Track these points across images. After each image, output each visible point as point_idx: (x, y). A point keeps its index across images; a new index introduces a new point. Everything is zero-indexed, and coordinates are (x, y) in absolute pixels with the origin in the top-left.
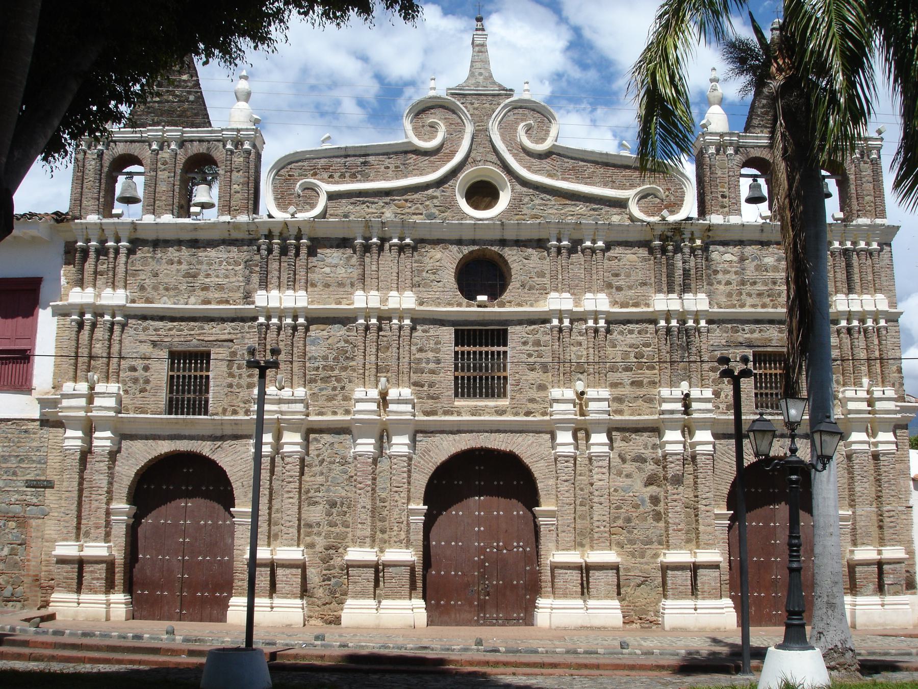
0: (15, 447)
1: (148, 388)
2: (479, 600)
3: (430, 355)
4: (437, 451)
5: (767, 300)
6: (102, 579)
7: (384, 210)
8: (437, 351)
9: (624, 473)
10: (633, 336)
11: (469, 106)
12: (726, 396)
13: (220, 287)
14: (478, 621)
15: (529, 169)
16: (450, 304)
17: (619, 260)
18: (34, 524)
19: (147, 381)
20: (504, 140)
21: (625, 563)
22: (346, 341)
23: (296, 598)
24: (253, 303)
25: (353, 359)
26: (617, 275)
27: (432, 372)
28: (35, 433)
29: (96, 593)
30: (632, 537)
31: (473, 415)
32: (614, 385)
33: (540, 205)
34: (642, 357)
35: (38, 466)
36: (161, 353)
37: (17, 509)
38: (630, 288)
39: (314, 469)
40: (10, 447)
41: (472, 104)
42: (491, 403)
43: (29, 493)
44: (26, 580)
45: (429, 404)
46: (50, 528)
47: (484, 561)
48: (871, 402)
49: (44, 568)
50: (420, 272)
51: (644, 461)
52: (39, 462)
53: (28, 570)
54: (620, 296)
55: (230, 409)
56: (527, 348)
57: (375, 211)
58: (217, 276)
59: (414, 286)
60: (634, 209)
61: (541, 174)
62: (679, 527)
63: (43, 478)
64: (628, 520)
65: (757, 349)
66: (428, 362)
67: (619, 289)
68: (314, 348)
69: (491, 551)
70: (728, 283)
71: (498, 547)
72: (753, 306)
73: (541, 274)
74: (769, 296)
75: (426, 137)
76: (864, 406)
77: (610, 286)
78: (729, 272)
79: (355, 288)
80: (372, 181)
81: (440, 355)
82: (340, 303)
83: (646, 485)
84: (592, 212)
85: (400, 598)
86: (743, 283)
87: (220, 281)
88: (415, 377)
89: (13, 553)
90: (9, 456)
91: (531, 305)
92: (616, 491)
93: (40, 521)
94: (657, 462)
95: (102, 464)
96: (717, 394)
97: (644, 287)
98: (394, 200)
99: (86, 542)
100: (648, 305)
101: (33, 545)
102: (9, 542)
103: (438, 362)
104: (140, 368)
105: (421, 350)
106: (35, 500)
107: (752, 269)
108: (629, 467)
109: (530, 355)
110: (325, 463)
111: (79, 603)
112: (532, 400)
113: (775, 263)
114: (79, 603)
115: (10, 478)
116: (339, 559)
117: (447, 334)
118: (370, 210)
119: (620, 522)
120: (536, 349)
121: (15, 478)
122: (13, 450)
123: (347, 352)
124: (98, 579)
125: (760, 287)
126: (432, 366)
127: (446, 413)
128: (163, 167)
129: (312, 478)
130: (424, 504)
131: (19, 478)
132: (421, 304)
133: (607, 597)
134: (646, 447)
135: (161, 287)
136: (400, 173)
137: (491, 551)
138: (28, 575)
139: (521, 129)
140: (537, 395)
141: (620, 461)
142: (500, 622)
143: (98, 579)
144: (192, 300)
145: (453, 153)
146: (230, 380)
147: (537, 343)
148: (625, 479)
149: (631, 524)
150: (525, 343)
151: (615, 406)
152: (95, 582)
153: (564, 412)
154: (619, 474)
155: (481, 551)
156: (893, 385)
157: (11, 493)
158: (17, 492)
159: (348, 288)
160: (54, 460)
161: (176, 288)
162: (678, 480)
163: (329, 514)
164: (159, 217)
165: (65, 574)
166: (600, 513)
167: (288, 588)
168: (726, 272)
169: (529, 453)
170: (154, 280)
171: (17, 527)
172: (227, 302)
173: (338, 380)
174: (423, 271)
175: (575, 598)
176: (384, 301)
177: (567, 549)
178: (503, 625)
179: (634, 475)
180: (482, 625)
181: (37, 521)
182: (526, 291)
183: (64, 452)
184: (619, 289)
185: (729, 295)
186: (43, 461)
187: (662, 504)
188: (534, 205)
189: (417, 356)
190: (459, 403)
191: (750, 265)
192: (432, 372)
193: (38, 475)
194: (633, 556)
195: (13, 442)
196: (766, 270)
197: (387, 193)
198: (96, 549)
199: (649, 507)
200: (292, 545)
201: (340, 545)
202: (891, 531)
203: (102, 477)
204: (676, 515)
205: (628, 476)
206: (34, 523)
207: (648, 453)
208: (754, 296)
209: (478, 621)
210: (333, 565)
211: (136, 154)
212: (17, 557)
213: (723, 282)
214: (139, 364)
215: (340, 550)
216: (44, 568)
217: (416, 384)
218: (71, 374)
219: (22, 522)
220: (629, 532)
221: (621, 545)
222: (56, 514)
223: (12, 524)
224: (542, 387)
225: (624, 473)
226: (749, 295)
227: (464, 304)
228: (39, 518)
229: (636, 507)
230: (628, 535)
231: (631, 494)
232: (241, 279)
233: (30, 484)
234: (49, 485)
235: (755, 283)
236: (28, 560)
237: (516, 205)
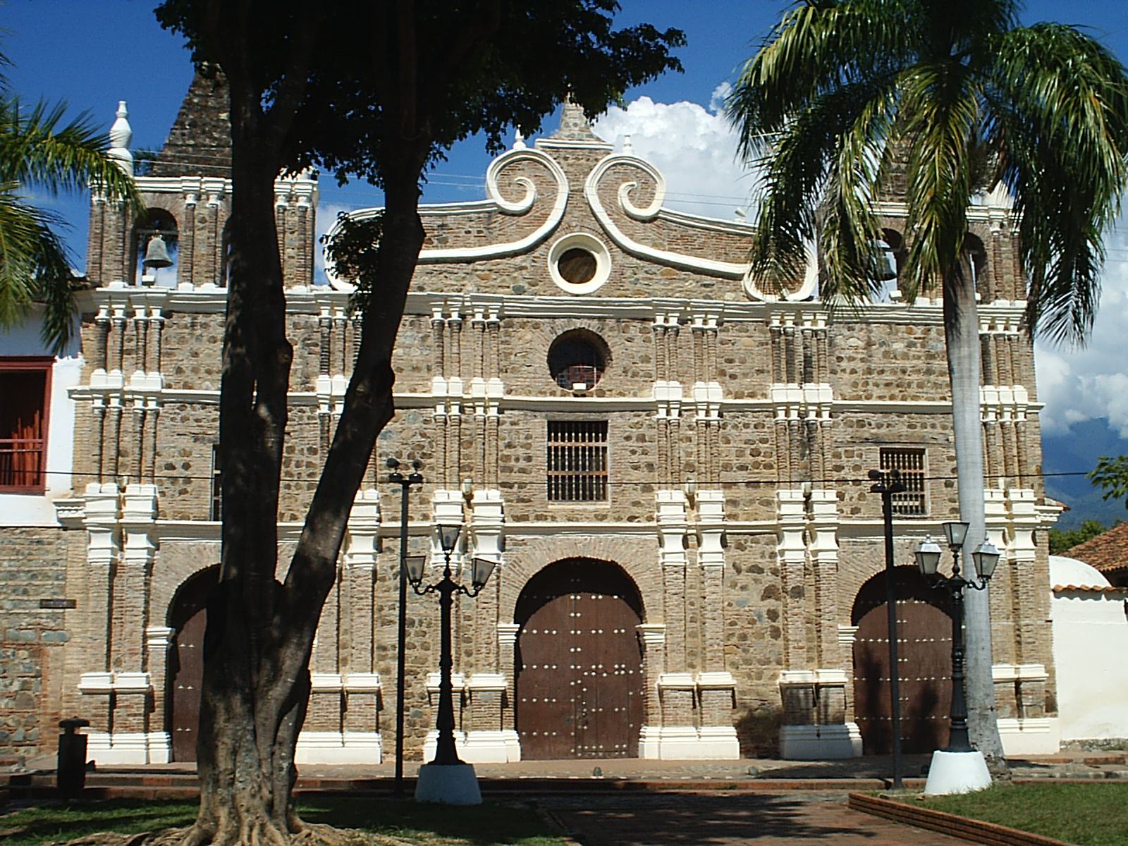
0: (25, 561)
1: (189, 489)
2: (576, 730)
3: (521, 452)
4: (529, 561)
5: (896, 391)
6: (140, 715)
7: (465, 282)
8: (528, 446)
9: (739, 585)
10: (748, 430)
11: (562, 161)
12: (851, 498)
14: (575, 753)
15: (631, 237)
16: (542, 393)
17: (733, 344)
18: (51, 652)
20: (603, 203)
21: (740, 686)
22: (423, 435)
23: (370, 731)
24: (313, 389)
25: (430, 456)
26: (731, 361)
27: (522, 471)
28: (50, 544)
29: (132, 731)
30: (748, 656)
32: (728, 485)
33: (644, 279)
34: (759, 455)
35: (56, 583)
36: (204, 448)
37: (30, 635)
38: (745, 375)
39: (386, 583)
40: (19, 560)
41: (566, 159)
42: (590, 506)
43: (44, 616)
44: (41, 719)
45: (520, 509)
46: (72, 656)
47: (581, 686)
48: (1008, 505)
49: (64, 705)
50: (508, 355)
51: (761, 571)
52: (57, 579)
53: (45, 707)
54: (734, 385)
56: (630, 443)
57: (455, 283)
59: (502, 371)
60: (749, 284)
61: (645, 244)
62: (800, 644)
63: (62, 597)
64: (744, 637)
65: (884, 446)
66: (517, 460)
67: (733, 377)
68: (385, 443)
69: (590, 675)
70: (853, 371)
71: (596, 670)
72: (880, 398)
73: (646, 359)
74: (898, 386)
75: (513, 197)
76: (1001, 509)
77: (722, 373)
78: (854, 359)
79: (432, 373)
80: (451, 247)
81: (531, 452)
82: (415, 391)
83: (762, 600)
84: (703, 288)
85: (490, 729)
86: (869, 371)
88: (503, 477)
89: (26, 685)
90: (18, 572)
91: (635, 395)
92: (730, 605)
94: (775, 572)
95: (137, 580)
96: (841, 496)
97: (761, 375)
98: (476, 270)
99: (117, 672)
100: (764, 396)
101: (50, 677)
103: (529, 459)
105: (509, 446)
106: (52, 624)
107: (880, 356)
108: (744, 578)
109: (633, 452)
112: (636, 504)
113: (905, 350)
114: (112, 745)
116: (419, 686)
117: (539, 426)
118: (449, 282)
119: (734, 640)
120: (640, 444)
121: (26, 598)
122: (23, 565)
123: (424, 447)
124: (135, 715)
125: (888, 377)
126: (522, 464)
127: (538, 518)
128: (201, 225)
129: (386, 594)
130: (515, 623)
132: (509, 392)
133: (721, 724)
134: (763, 556)
135: (203, 370)
136: (485, 237)
137: (590, 675)
138: (45, 714)
139: (623, 189)
140: (643, 498)
141: (734, 571)
142: (601, 754)
143: (135, 715)
145: (546, 216)
147: (642, 438)
148: (740, 592)
149: (748, 642)
150: (628, 438)
151: (730, 509)
152: (131, 718)
153: (673, 517)
154: (734, 585)
155: (578, 674)
156: (1032, 487)
159: (424, 373)
160: (75, 576)
162: (798, 593)
164: (199, 286)
165: (94, 711)
166: (714, 630)
167: (361, 721)
168: (851, 359)
169: (633, 564)
170: (194, 362)
171: (31, 656)
174: (511, 354)
175: (686, 725)
176: (467, 388)
177: (678, 671)
178: (604, 757)
179: (751, 587)
180: (580, 758)
182: (629, 378)
183: (89, 568)
184: (733, 377)
185: (855, 385)
187: (780, 619)
188: (638, 279)
189: (506, 452)
190: (555, 506)
191: (877, 351)
192: (522, 471)
193: (55, 593)
194: (749, 677)
195: (23, 554)
196: (895, 357)
197: (469, 261)
198: (132, 680)
199: (767, 622)
200: (365, 671)
201: (419, 670)
202: (1030, 646)
203: (137, 594)
204: (796, 630)
205: (743, 588)
206: (51, 650)
207: (764, 563)
208: (882, 386)
209: (575, 753)
210: (412, 693)
211: (167, 209)
213: (848, 371)
214: (178, 461)
216: (64, 705)
217: (503, 485)
219: (37, 651)
220: (744, 650)
221: (735, 665)
223: (23, 653)
224: (647, 488)
225: (739, 585)
226: (877, 385)
227: (559, 393)
229: (752, 622)
230: (743, 654)
231: (747, 609)
233: (44, 604)
234: (72, 605)
235: (882, 372)
236: (45, 696)
237: (616, 281)
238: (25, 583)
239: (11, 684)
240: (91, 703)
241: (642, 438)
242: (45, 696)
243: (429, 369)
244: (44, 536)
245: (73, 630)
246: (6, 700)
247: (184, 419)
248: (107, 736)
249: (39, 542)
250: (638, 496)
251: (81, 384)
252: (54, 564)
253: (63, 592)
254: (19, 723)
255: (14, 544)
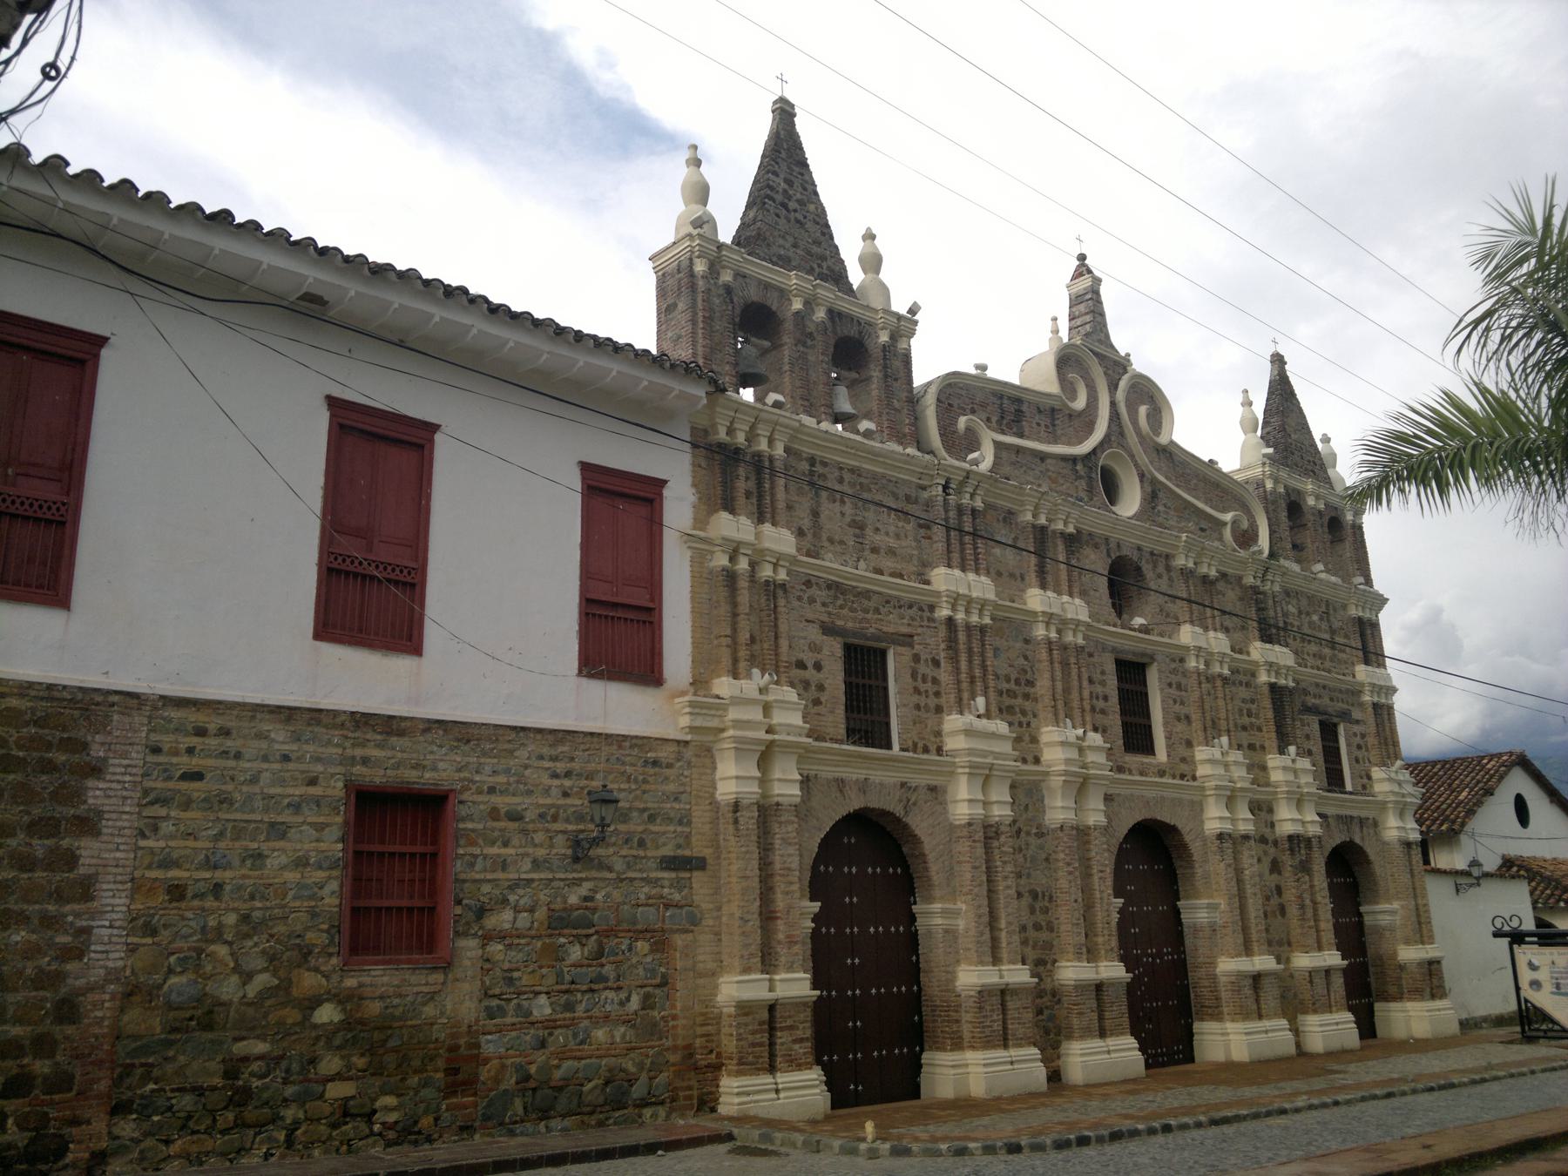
1: (823, 699)
13: (891, 552)
18: (679, 942)
19: (821, 688)
22: (1026, 658)
28: (670, 766)
31: (1141, 774)
35: (679, 829)
37: (647, 916)
43: (666, 883)
49: (700, 1031)
52: (680, 823)
55: (920, 745)
58: (887, 534)
63: (687, 853)
72: (1312, 668)
80: (1028, 438)
87: (892, 542)
89: (647, 1002)
93: (690, 937)
101: (679, 985)
102: (640, 983)
103: (1106, 698)
104: (810, 664)
106: (677, 897)
110: (1023, 834)
111: (777, 1091)
112: (1183, 760)
114: (777, 1091)
115: (634, 852)
121: (642, 853)
122: (636, 798)
124: (801, 1040)
131: (649, 854)
143: (801, 1040)
144: (862, 564)
146: (916, 699)
152: (797, 1047)
157: (636, 883)
158: (647, 881)
161: (842, 542)
163: (1032, 911)
165: (750, 1038)
167: (1021, 1032)
171: (652, 951)
172: (901, 576)
173: (1024, 713)
175: (1252, 1019)
181: (684, 936)
186: (684, 820)
193: (679, 846)
195: (636, 781)
212: (655, 1013)
214: (809, 658)
215: (1049, 966)
218: (726, 661)
219: (660, 945)
222: (711, 922)
223: (642, 946)
228: (687, 931)
232: (914, 544)
233: (671, 863)
234: (699, 864)
236: (674, 1017)
238: (640, 829)
239: (628, 999)
240: (746, 1025)
241: (1179, 687)
242: (674, 1017)
243: (1023, 579)
244: (664, 754)
245: (704, 906)
246: (622, 1029)
247: (812, 601)
248: (767, 1079)
249: (655, 763)
250: (1182, 751)
251: (694, 528)
252: (676, 799)
253: (688, 844)
254: (641, 1066)
255: (624, 763)
